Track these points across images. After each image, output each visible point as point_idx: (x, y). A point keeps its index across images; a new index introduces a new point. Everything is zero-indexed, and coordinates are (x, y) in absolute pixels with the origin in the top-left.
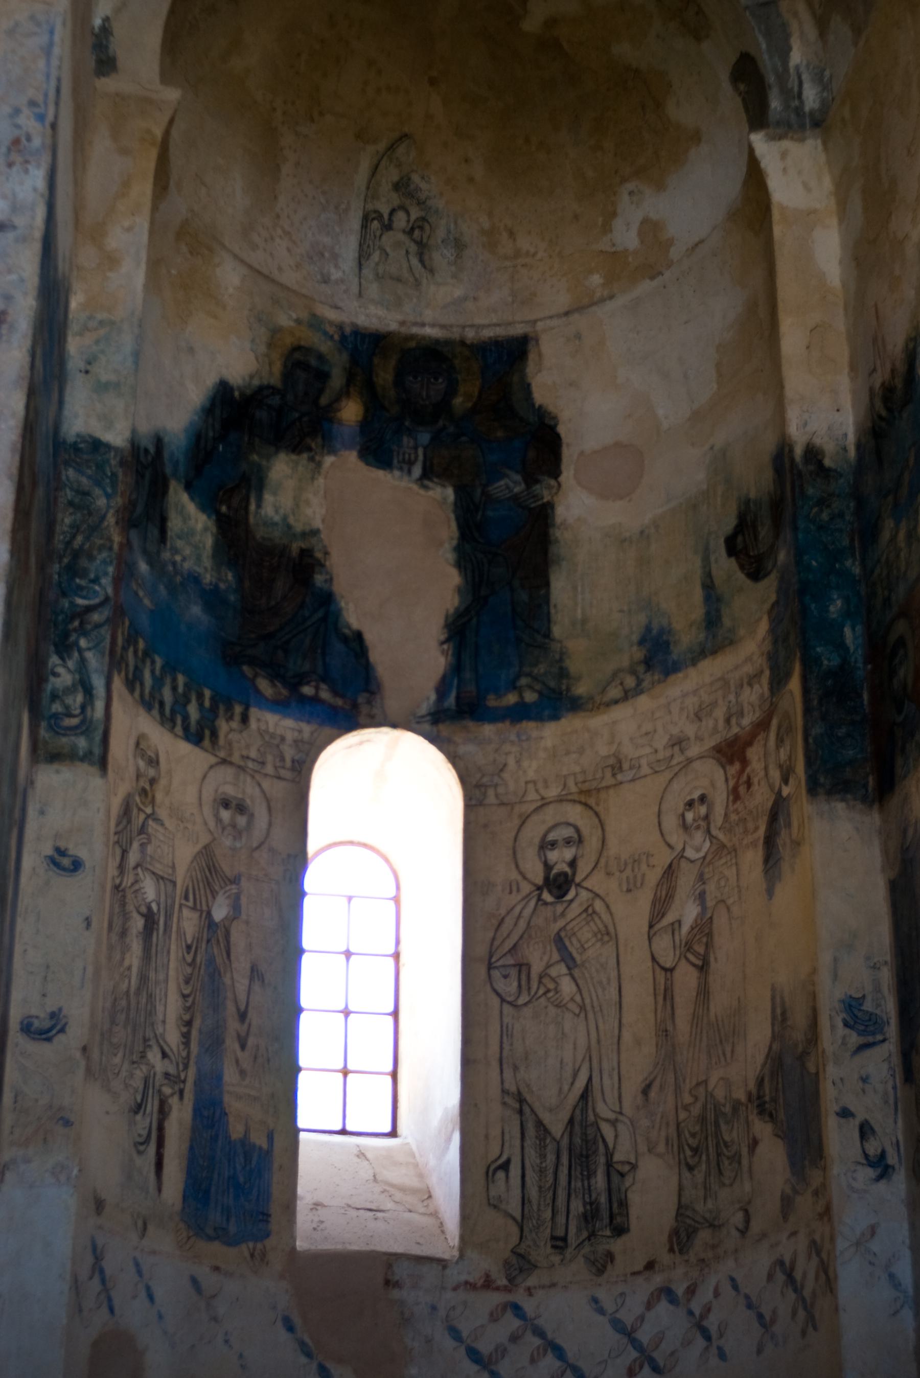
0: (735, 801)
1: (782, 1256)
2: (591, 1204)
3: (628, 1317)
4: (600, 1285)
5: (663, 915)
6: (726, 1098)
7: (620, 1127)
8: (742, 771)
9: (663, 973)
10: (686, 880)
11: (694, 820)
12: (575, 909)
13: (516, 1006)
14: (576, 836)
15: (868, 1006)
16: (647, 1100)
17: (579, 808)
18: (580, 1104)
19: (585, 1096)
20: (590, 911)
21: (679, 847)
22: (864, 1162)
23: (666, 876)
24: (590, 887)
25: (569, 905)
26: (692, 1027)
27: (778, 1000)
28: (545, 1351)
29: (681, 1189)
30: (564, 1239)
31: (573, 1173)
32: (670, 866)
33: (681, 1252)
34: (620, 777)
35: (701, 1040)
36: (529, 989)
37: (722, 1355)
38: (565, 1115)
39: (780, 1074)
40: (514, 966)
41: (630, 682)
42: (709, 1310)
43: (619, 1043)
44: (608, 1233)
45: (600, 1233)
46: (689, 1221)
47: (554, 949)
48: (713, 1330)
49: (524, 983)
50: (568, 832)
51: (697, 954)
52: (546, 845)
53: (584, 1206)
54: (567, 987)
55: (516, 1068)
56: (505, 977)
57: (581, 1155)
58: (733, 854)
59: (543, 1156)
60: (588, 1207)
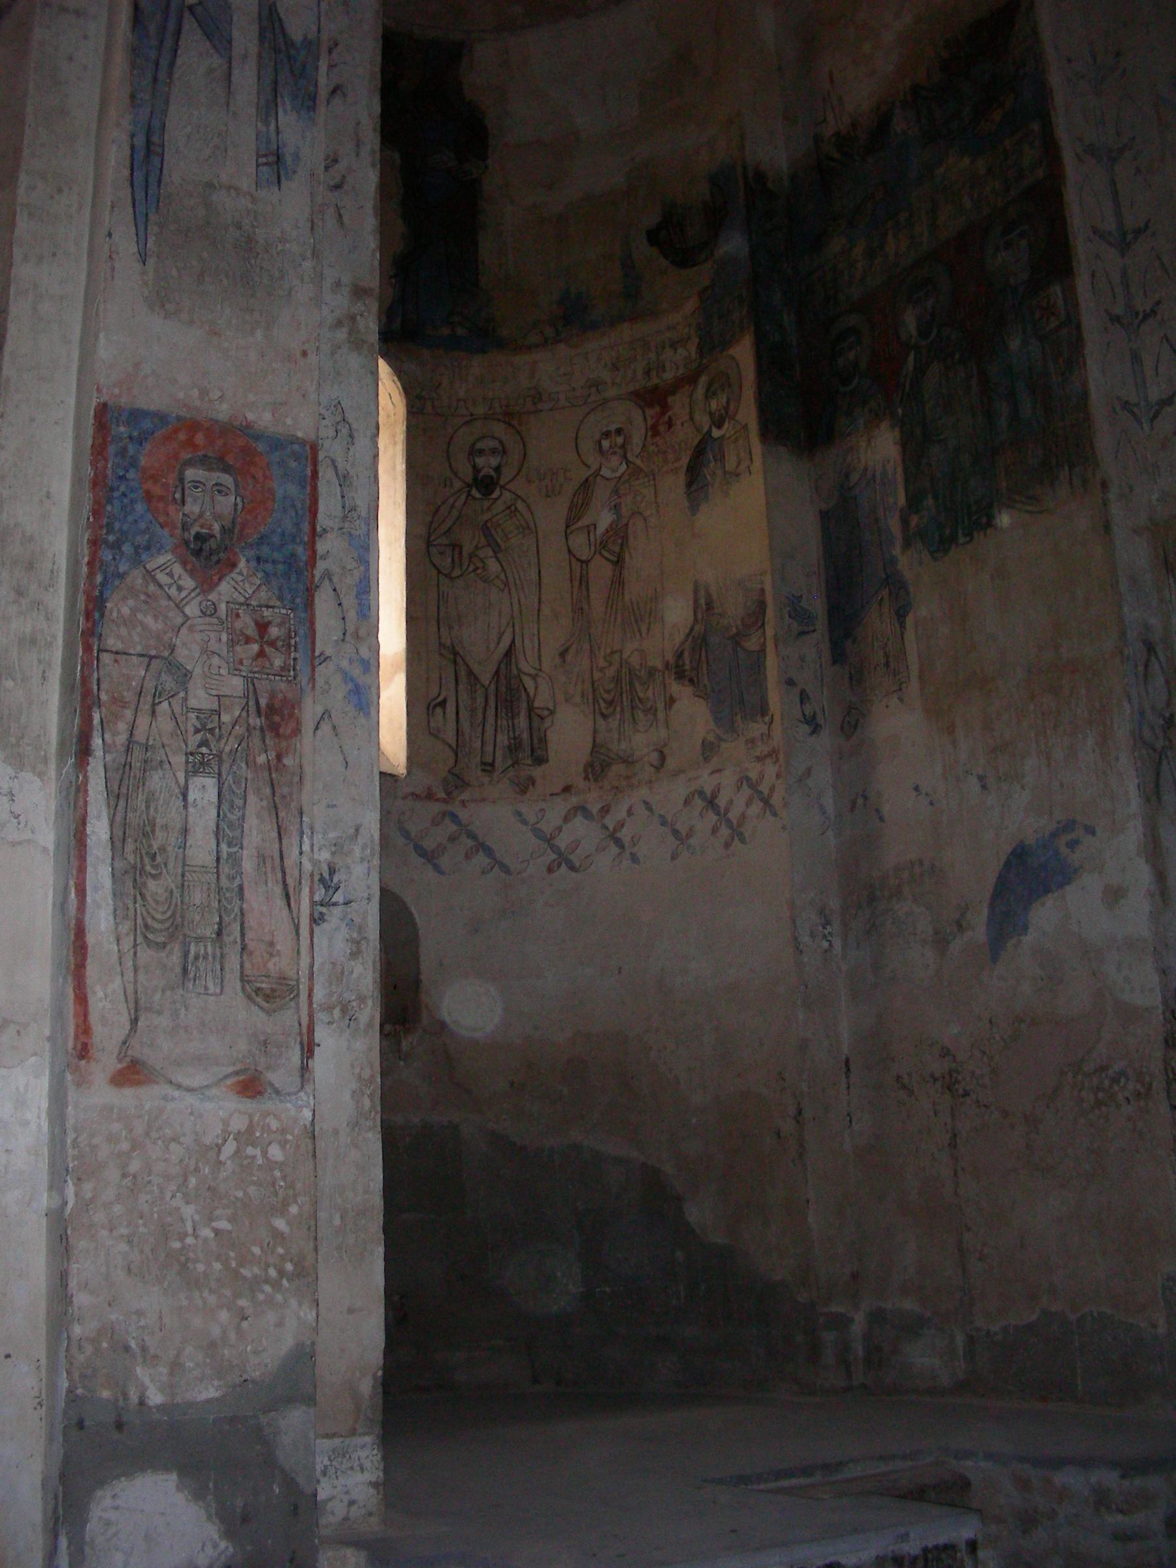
0: (653, 436)
1: (702, 788)
2: (515, 738)
3: (547, 827)
4: (523, 802)
5: (579, 519)
6: (641, 664)
7: (539, 680)
8: (663, 413)
9: (579, 564)
10: (601, 493)
11: (611, 447)
12: (499, 506)
13: (451, 578)
14: (501, 448)
15: (804, 604)
16: (564, 661)
17: (503, 426)
18: (505, 661)
19: (509, 653)
20: (513, 508)
21: (595, 467)
22: (802, 719)
23: (582, 488)
24: (513, 489)
25: (492, 504)
26: (607, 607)
27: (702, 593)
28: (478, 851)
29: (595, 732)
30: (492, 765)
31: (499, 715)
32: (587, 480)
33: (596, 780)
34: (539, 406)
35: (615, 619)
36: (461, 565)
37: (634, 858)
38: (492, 668)
39: (703, 650)
40: (449, 545)
41: (549, 332)
42: (623, 825)
43: (538, 615)
44: (529, 762)
45: (523, 762)
46: (602, 757)
47: (481, 534)
48: (626, 840)
49: (456, 560)
50: (492, 444)
51: (612, 552)
52: (473, 452)
53: (509, 741)
54: (493, 566)
55: (450, 627)
56: (441, 553)
57: (506, 700)
58: (651, 477)
59: (474, 699)
60: (512, 741)
